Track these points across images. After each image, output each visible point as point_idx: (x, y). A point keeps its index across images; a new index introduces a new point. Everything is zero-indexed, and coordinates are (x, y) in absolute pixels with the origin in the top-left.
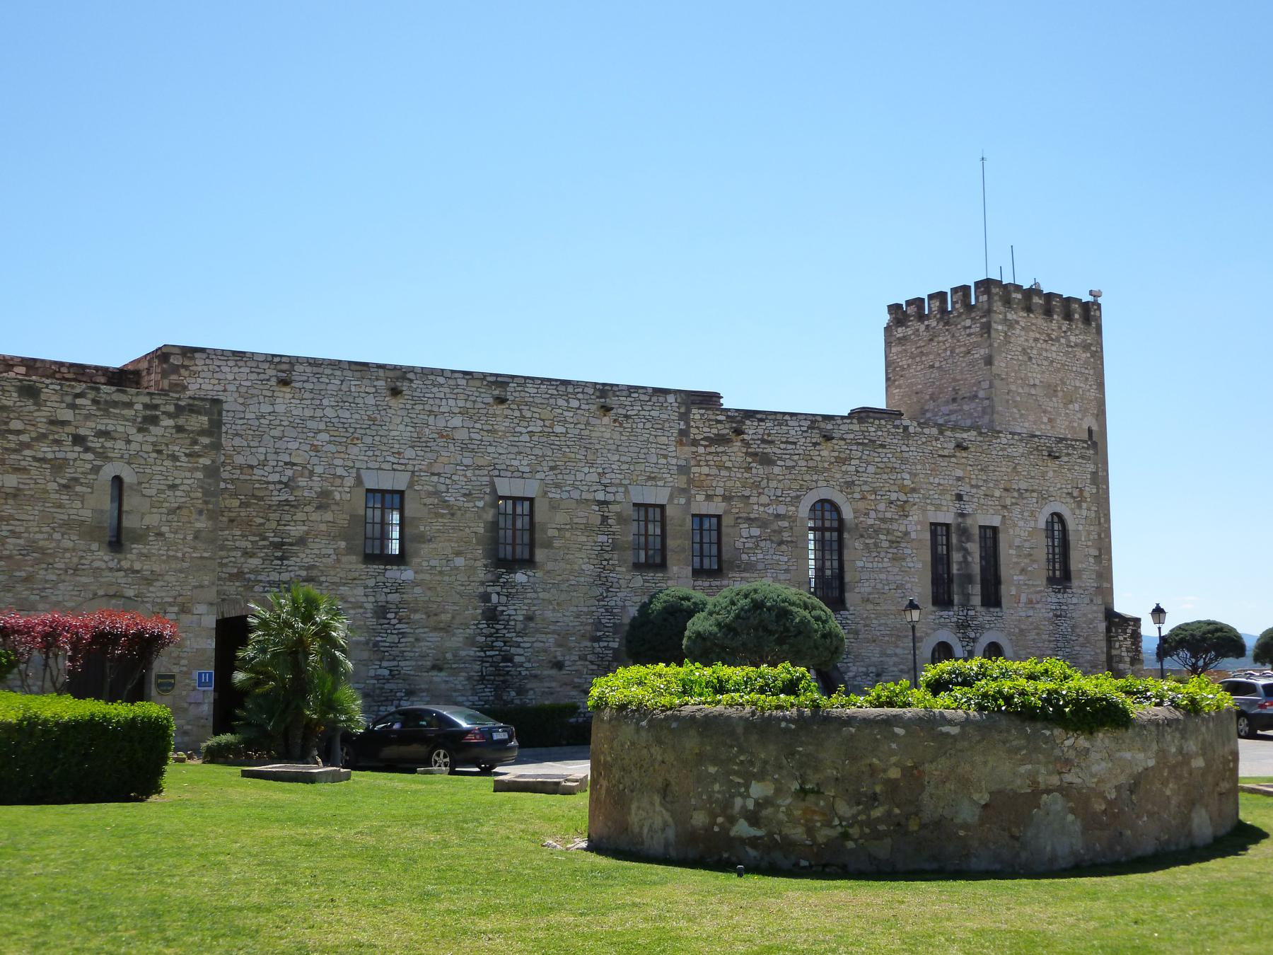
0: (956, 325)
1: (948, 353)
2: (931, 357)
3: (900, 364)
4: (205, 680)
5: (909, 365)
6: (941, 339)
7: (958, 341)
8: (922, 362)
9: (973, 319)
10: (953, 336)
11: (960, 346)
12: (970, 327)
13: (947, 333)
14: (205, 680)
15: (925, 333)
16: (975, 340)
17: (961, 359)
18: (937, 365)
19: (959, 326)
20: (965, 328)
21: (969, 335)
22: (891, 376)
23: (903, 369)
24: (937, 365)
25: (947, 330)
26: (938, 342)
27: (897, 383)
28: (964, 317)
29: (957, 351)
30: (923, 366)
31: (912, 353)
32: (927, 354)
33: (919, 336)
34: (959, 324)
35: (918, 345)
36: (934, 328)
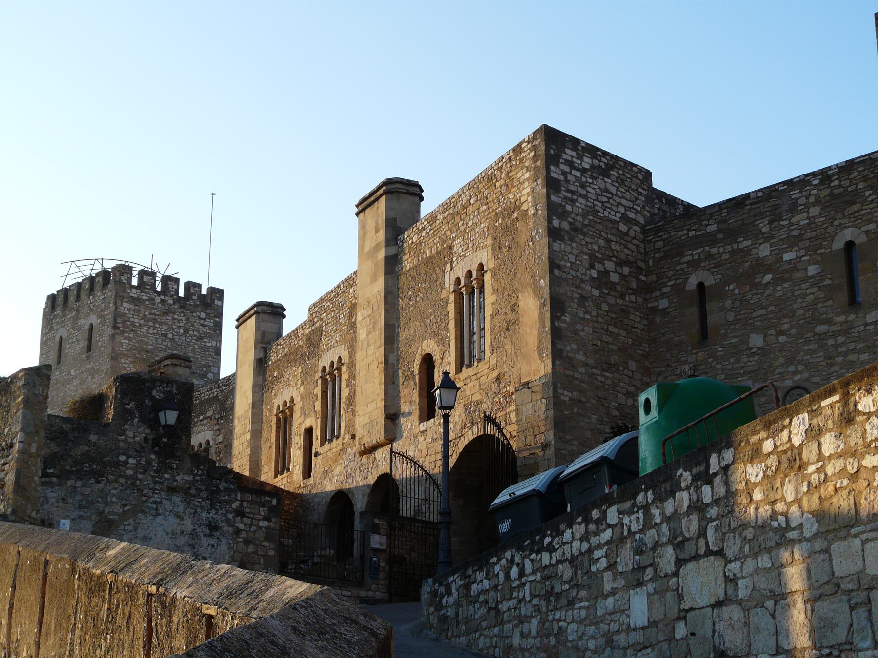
0: (192, 313)
1: (182, 331)
2: (165, 327)
3: (132, 320)
4: (793, 194)
5: (140, 325)
6: (176, 316)
7: (193, 326)
8: (155, 328)
9: (207, 314)
10: (188, 320)
11: (194, 331)
12: (205, 320)
13: (182, 315)
14: (793, 194)
15: (160, 305)
16: (208, 331)
17: (193, 341)
18: (170, 336)
19: (194, 314)
20: (200, 318)
21: (203, 325)
22: (120, 325)
23: (134, 326)
24: (170, 336)
25: (183, 312)
26: (173, 319)
27: (126, 335)
28: (199, 309)
29: (191, 333)
30: (155, 332)
31: (145, 315)
32: (161, 324)
33: (155, 304)
34: (195, 312)
35: (153, 312)
36: (170, 305)
